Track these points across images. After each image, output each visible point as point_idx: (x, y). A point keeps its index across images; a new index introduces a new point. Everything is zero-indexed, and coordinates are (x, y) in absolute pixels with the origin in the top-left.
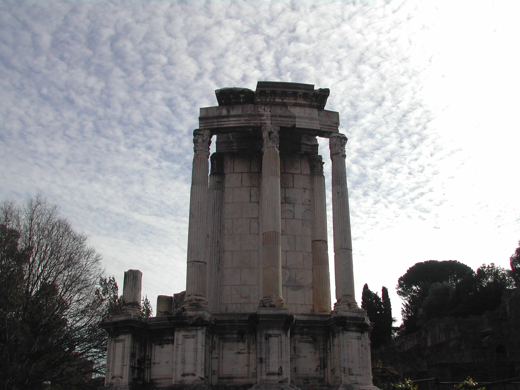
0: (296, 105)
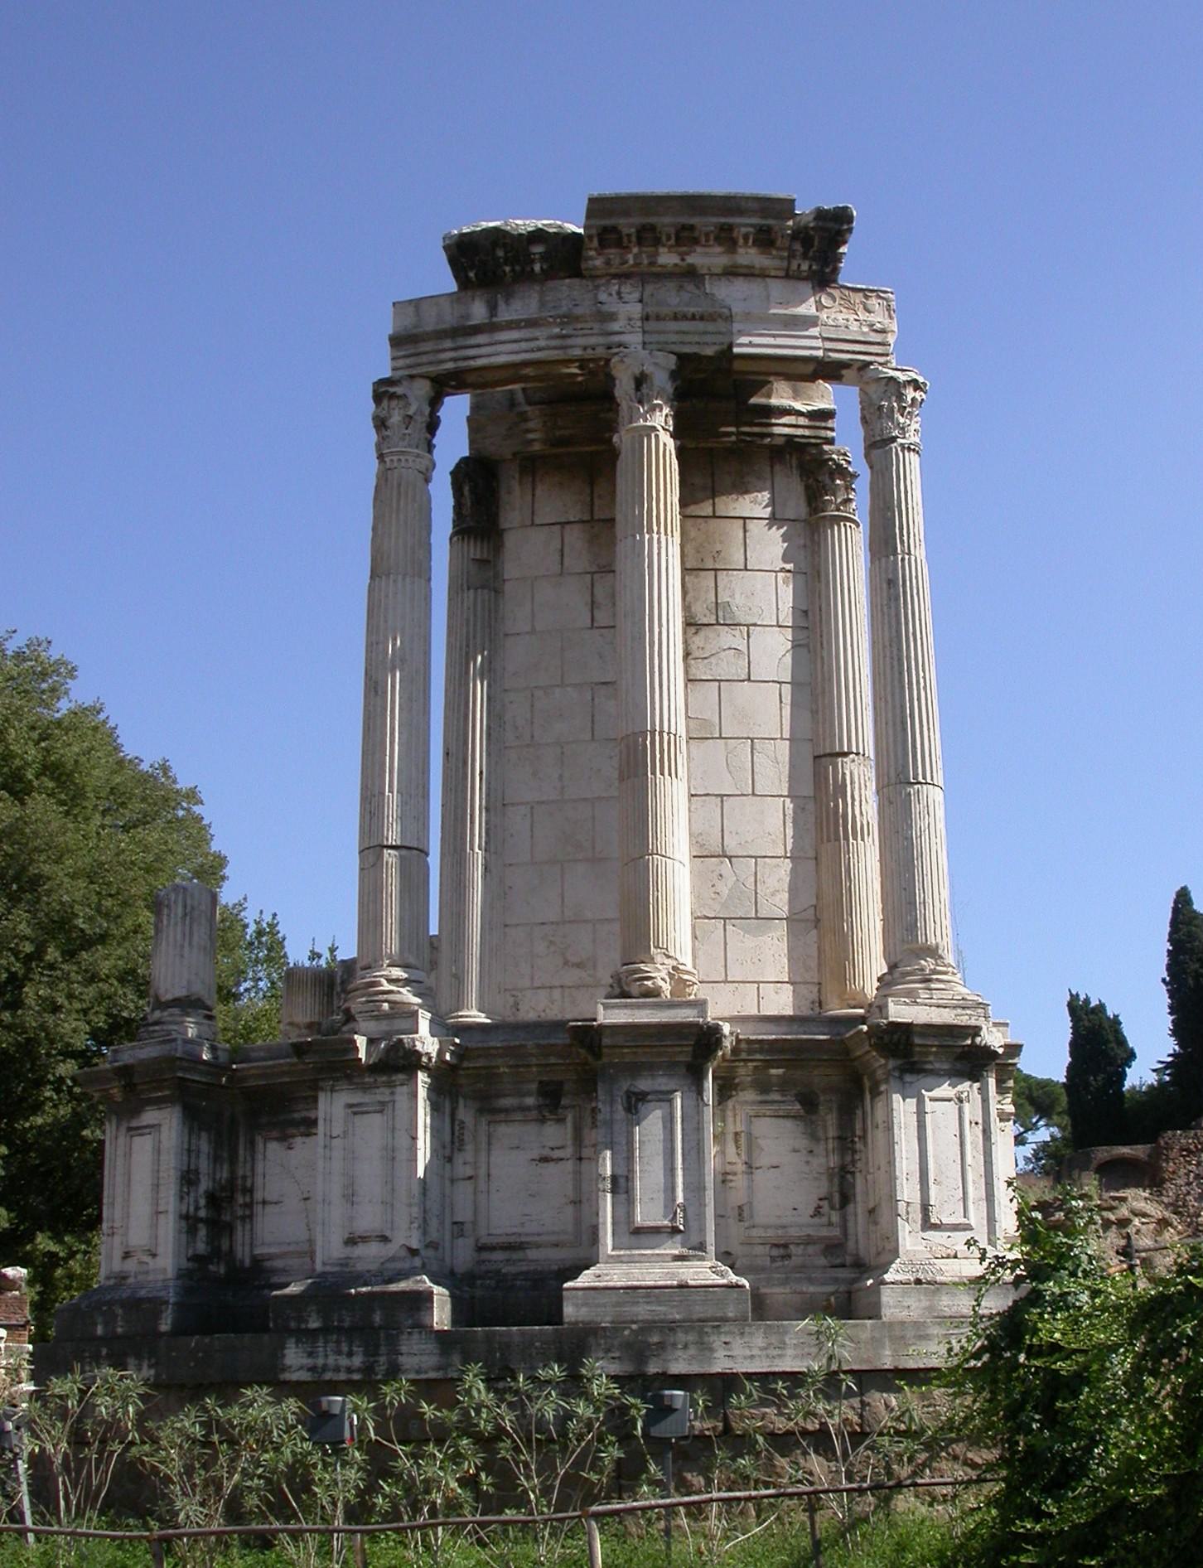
0: (731, 273)
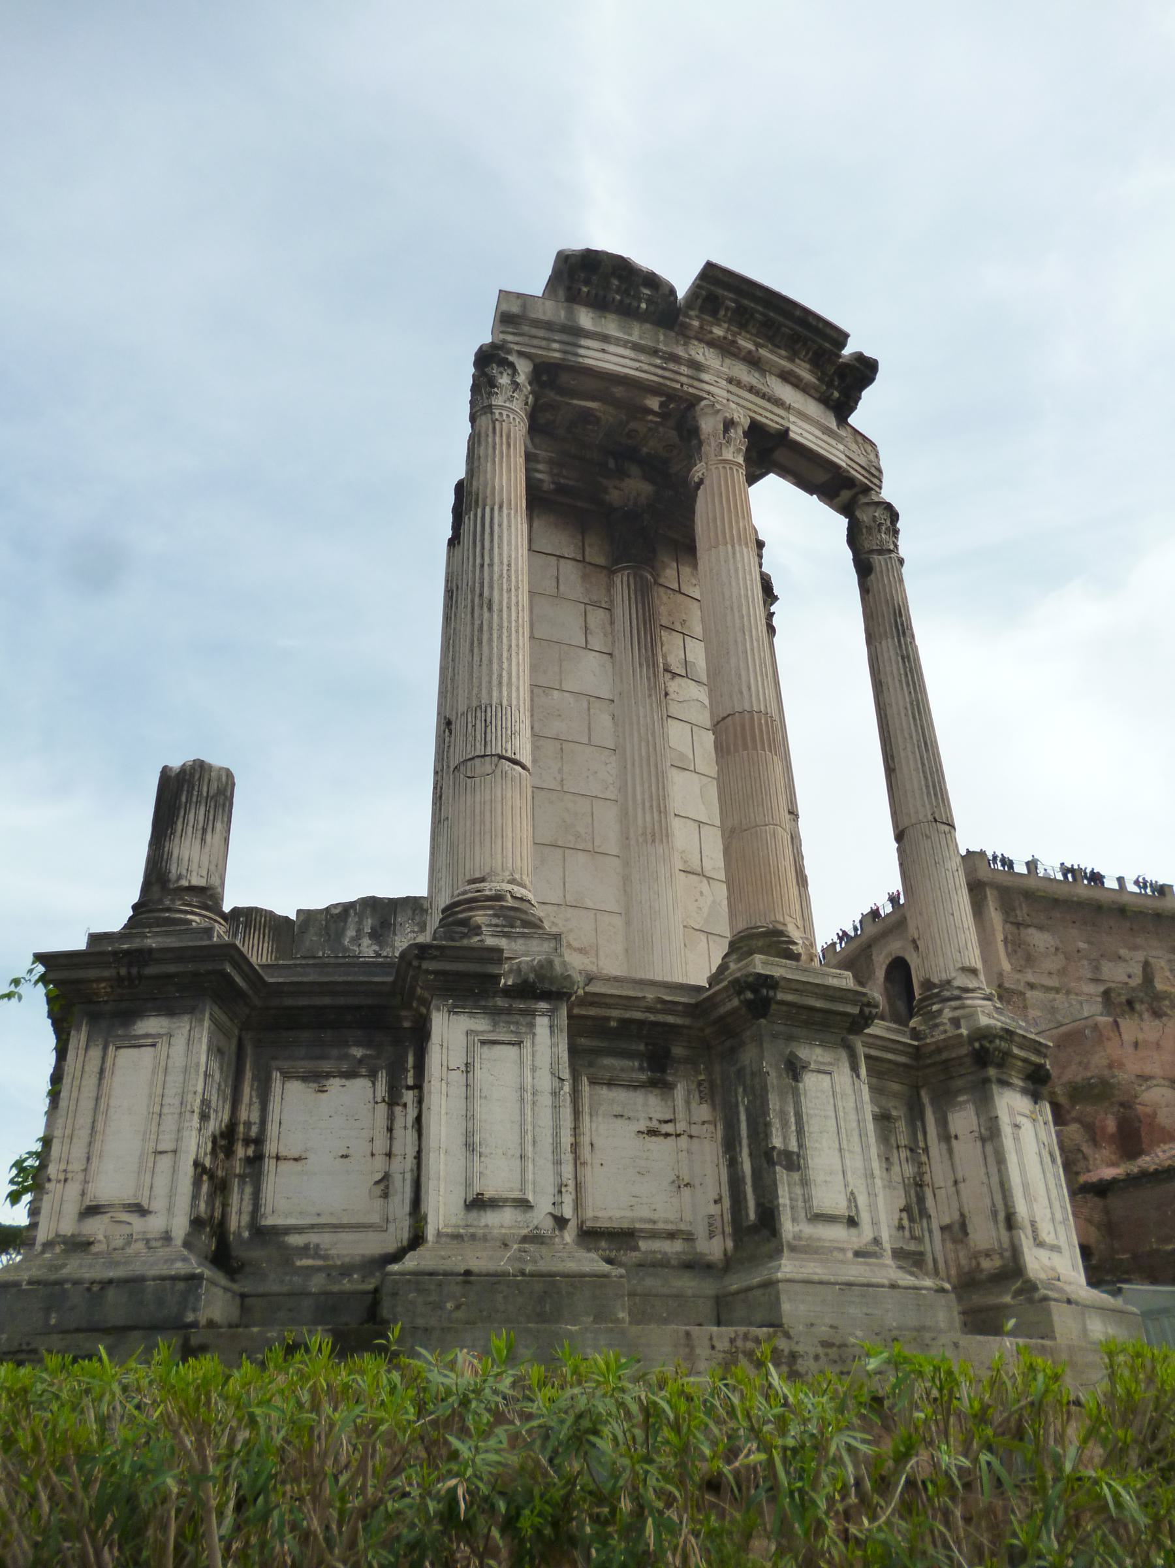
0: (786, 377)
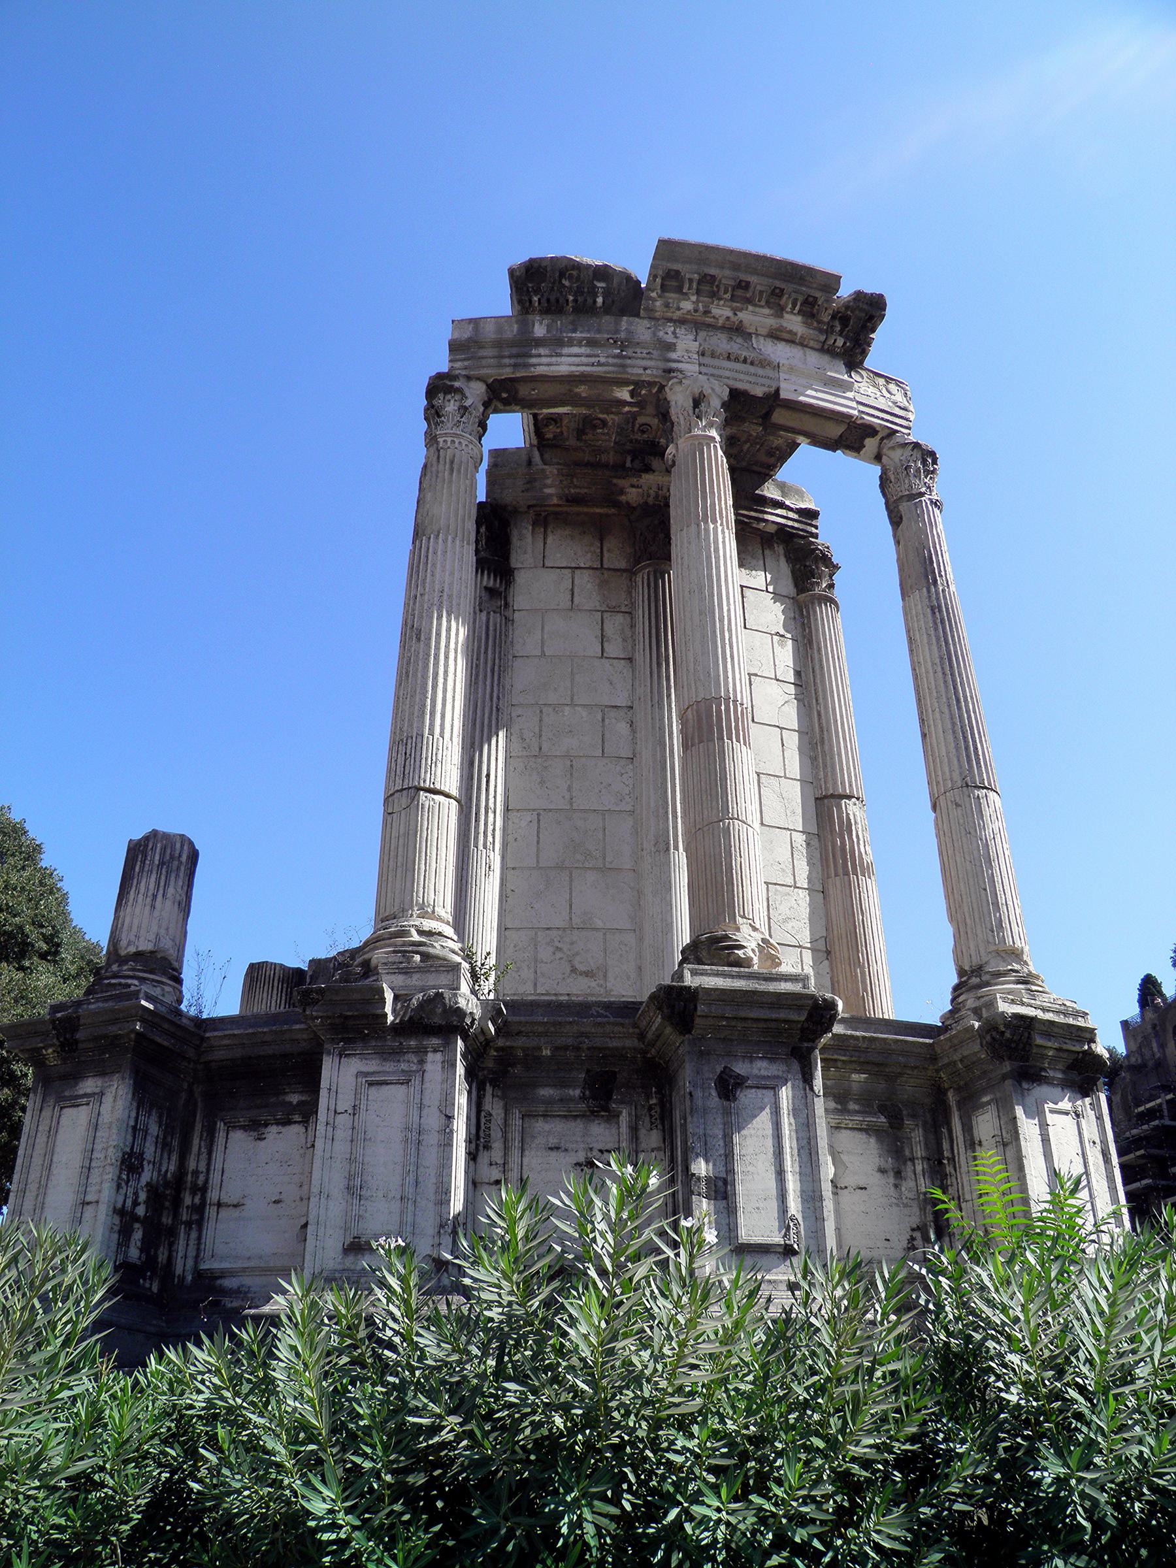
0: (775, 335)
